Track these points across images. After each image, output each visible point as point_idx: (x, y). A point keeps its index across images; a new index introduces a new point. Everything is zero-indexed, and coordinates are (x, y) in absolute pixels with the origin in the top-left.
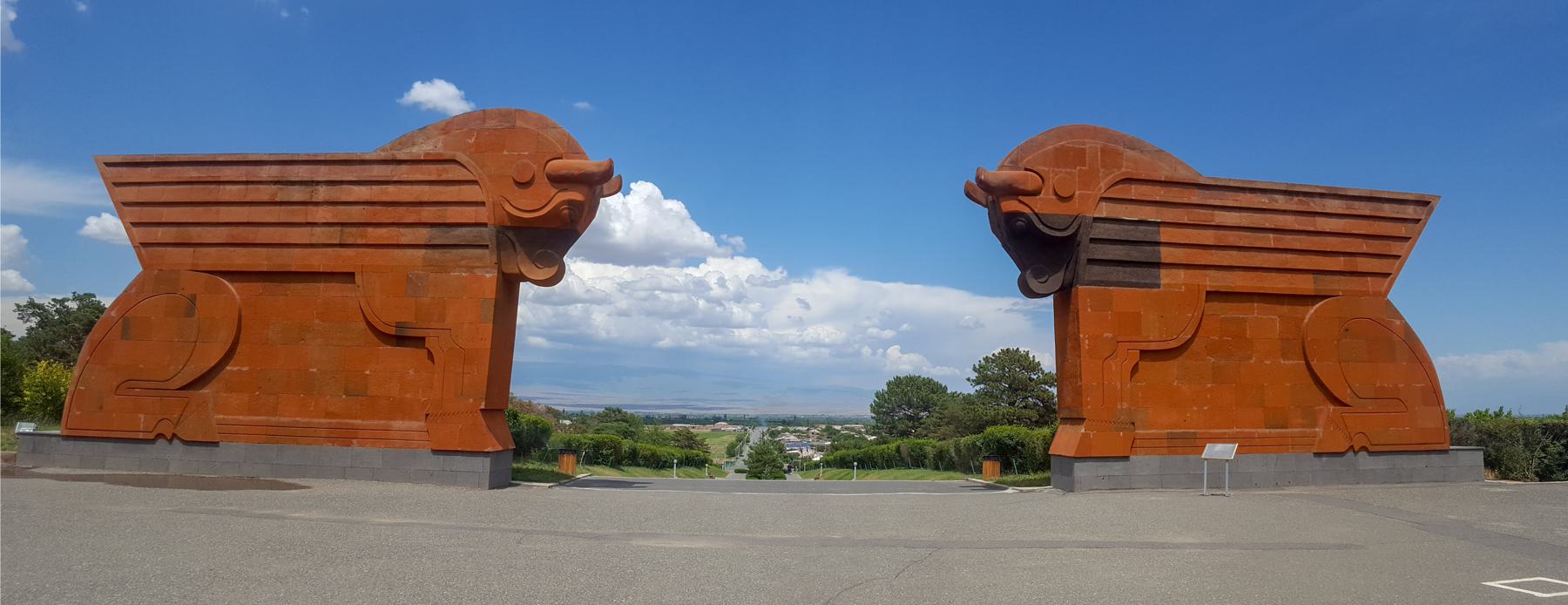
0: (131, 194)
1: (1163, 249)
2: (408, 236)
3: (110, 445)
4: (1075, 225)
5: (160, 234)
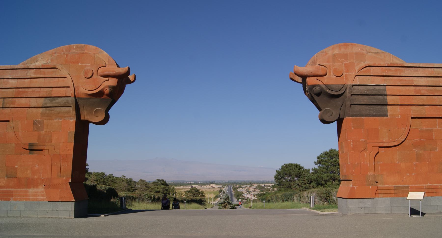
1: (388, 97)
2: (33, 103)
4: (344, 89)
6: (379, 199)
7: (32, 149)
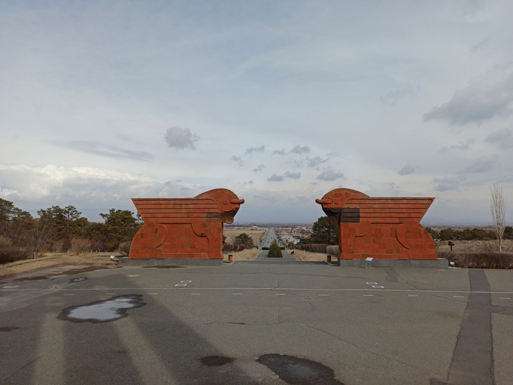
0: (141, 207)
2: (202, 215)
3: (140, 260)
5: (148, 215)
6: (355, 259)
7: (202, 236)
